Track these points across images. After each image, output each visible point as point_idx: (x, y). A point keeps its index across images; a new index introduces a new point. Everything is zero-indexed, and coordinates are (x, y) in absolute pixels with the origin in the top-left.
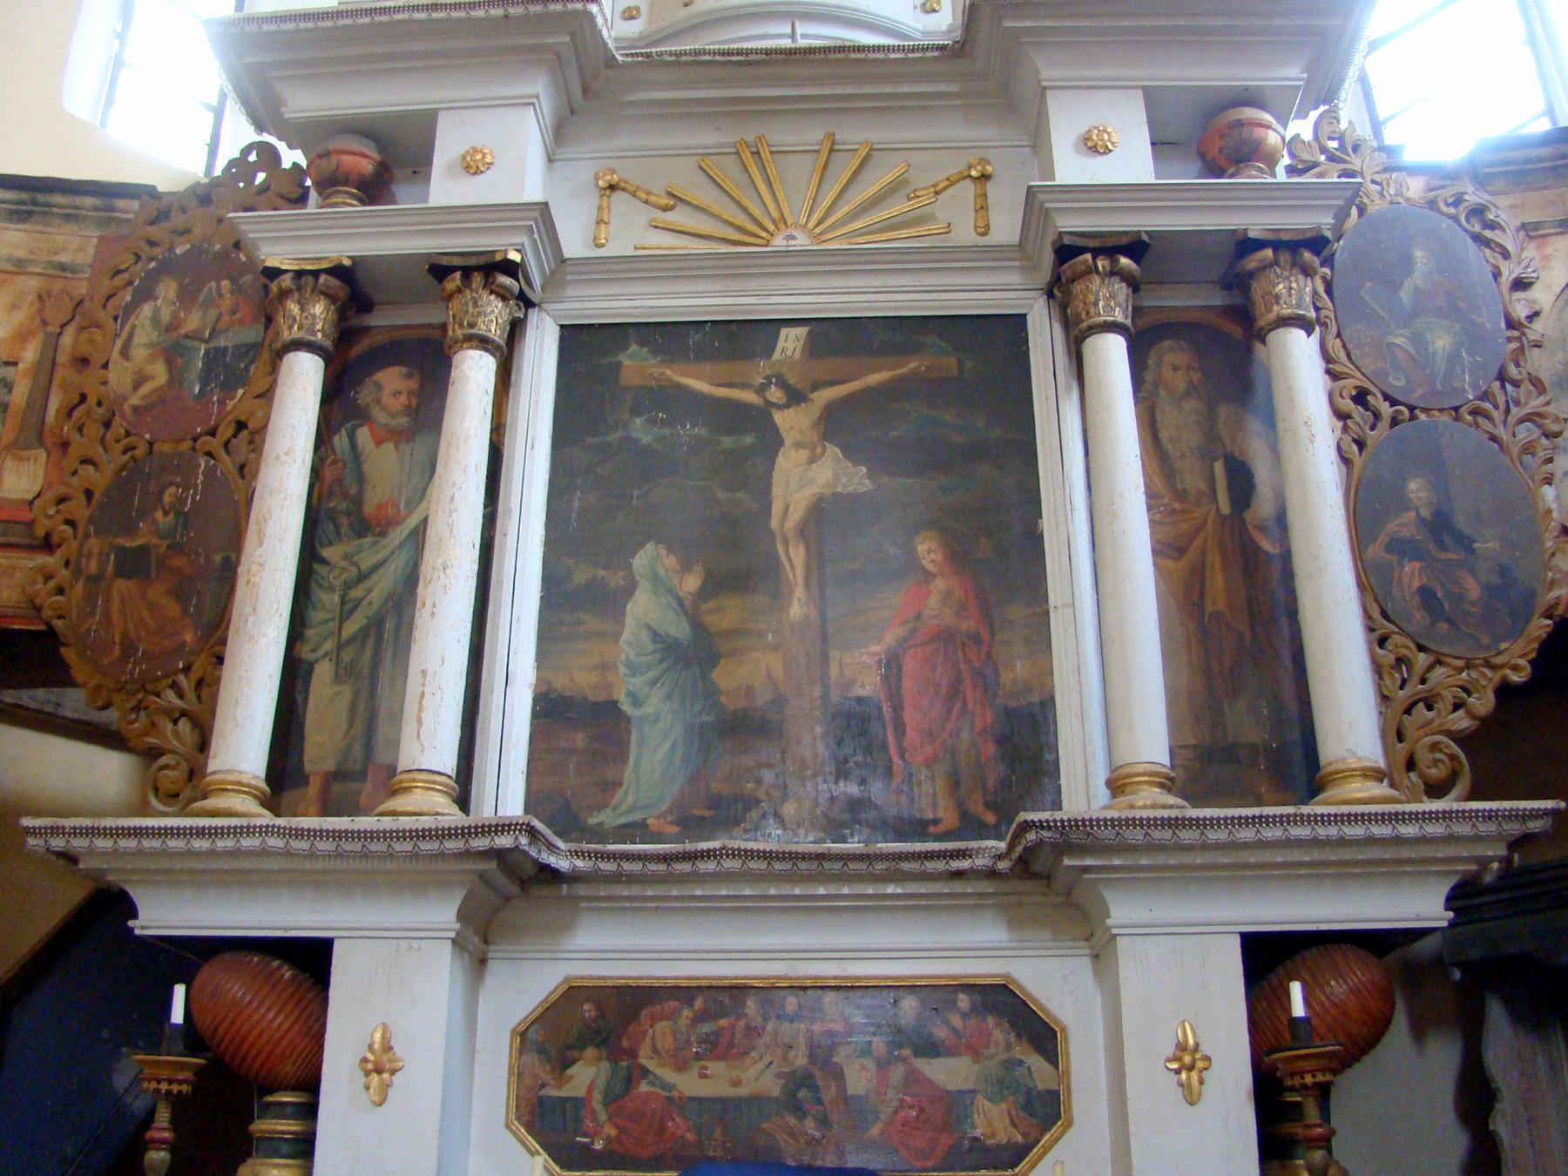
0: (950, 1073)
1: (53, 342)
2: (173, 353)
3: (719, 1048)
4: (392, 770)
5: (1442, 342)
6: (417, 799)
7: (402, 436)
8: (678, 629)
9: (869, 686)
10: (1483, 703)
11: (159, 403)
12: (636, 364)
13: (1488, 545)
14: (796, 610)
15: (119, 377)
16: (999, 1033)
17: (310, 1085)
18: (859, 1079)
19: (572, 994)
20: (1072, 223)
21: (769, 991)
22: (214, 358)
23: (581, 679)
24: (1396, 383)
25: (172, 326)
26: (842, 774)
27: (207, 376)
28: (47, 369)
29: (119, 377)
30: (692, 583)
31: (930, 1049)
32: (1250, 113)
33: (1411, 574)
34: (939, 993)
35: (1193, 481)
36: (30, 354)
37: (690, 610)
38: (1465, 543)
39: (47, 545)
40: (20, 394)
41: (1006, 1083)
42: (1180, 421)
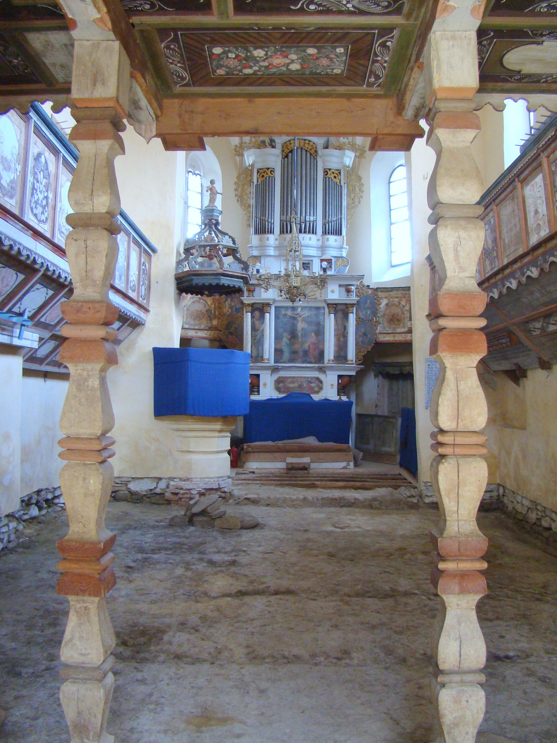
0: (313, 385)
1: (215, 305)
2: (231, 308)
3: (293, 382)
4: (262, 357)
5: (369, 312)
6: (266, 361)
7: (259, 320)
8: (288, 342)
9: (307, 348)
10: (365, 352)
11: (231, 314)
12: (283, 312)
13: (369, 336)
14: (300, 340)
15: (225, 310)
16: (317, 382)
17: (259, 386)
18: (305, 385)
19: (280, 378)
20: (329, 302)
21: (298, 377)
22: (236, 309)
23: (279, 347)
24: (363, 317)
25: (231, 305)
26: (304, 357)
27: (236, 311)
28: (215, 308)
29: (225, 310)
30: (289, 337)
31: (311, 383)
32: (350, 287)
33: (361, 339)
34: (312, 378)
35: (340, 328)
36: (213, 306)
37: (290, 340)
38: (367, 336)
39: (220, 331)
40: (213, 311)
41: (318, 386)
42: (340, 322)
